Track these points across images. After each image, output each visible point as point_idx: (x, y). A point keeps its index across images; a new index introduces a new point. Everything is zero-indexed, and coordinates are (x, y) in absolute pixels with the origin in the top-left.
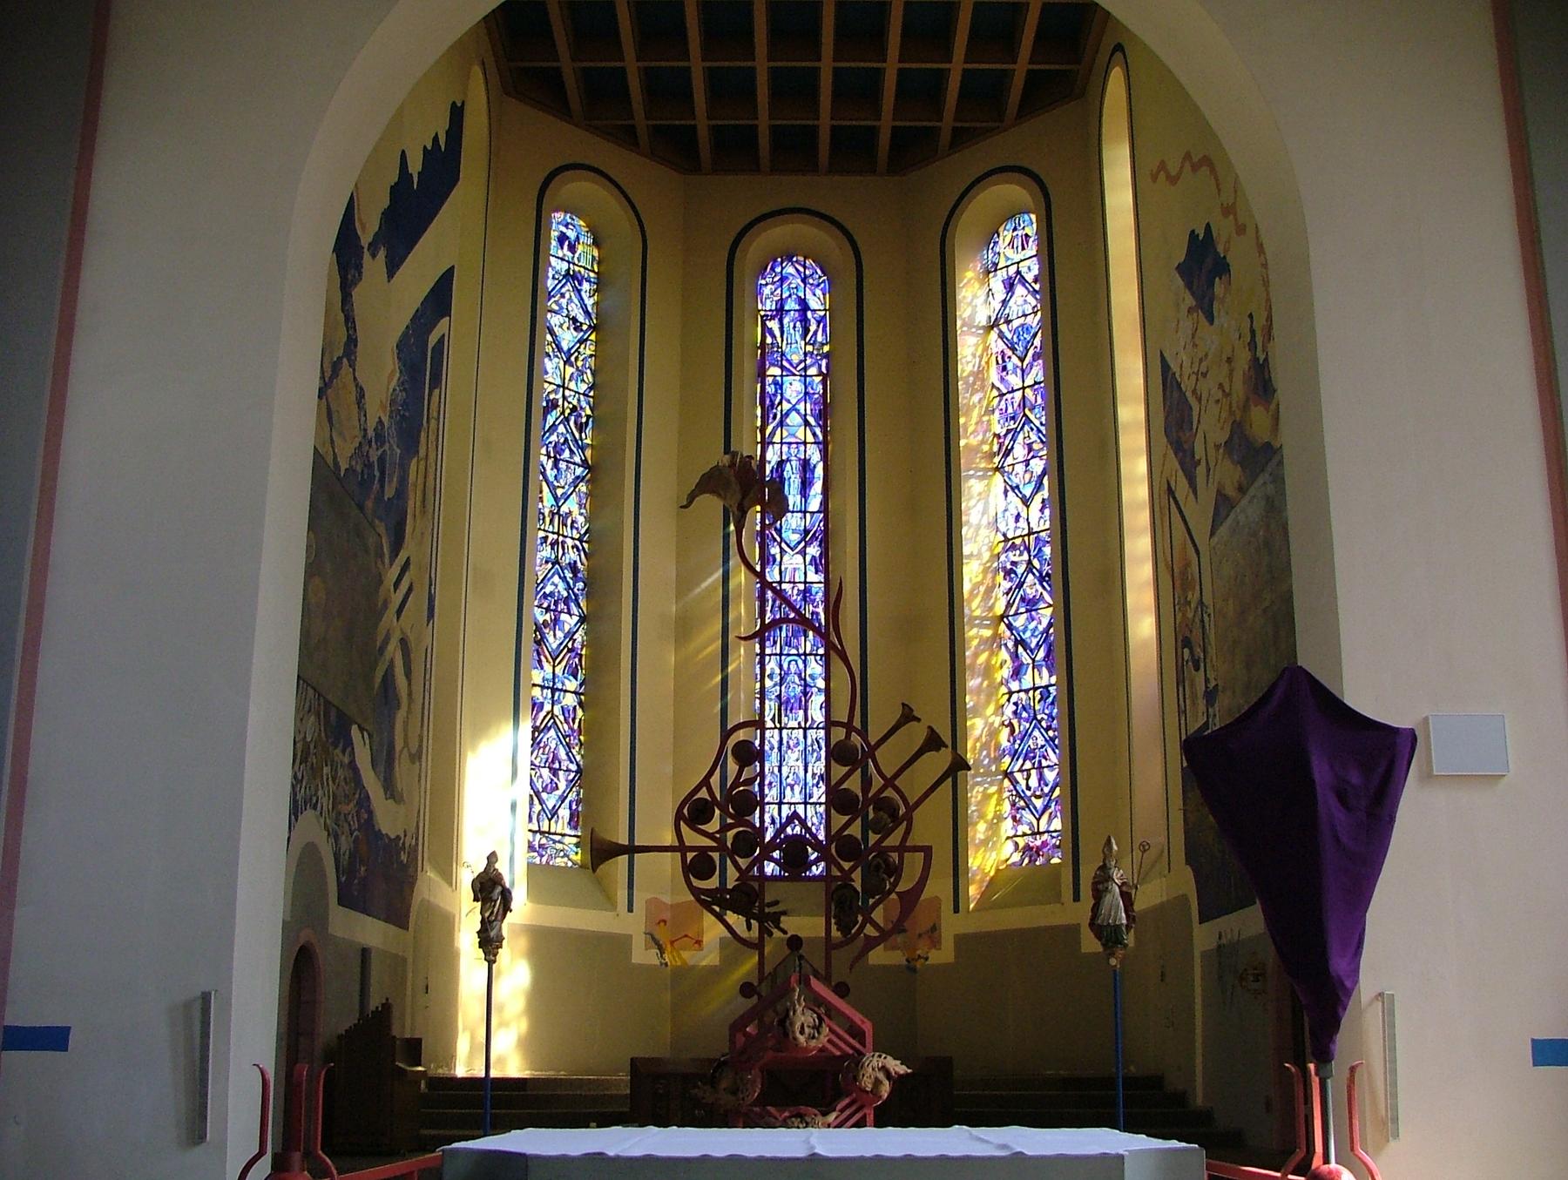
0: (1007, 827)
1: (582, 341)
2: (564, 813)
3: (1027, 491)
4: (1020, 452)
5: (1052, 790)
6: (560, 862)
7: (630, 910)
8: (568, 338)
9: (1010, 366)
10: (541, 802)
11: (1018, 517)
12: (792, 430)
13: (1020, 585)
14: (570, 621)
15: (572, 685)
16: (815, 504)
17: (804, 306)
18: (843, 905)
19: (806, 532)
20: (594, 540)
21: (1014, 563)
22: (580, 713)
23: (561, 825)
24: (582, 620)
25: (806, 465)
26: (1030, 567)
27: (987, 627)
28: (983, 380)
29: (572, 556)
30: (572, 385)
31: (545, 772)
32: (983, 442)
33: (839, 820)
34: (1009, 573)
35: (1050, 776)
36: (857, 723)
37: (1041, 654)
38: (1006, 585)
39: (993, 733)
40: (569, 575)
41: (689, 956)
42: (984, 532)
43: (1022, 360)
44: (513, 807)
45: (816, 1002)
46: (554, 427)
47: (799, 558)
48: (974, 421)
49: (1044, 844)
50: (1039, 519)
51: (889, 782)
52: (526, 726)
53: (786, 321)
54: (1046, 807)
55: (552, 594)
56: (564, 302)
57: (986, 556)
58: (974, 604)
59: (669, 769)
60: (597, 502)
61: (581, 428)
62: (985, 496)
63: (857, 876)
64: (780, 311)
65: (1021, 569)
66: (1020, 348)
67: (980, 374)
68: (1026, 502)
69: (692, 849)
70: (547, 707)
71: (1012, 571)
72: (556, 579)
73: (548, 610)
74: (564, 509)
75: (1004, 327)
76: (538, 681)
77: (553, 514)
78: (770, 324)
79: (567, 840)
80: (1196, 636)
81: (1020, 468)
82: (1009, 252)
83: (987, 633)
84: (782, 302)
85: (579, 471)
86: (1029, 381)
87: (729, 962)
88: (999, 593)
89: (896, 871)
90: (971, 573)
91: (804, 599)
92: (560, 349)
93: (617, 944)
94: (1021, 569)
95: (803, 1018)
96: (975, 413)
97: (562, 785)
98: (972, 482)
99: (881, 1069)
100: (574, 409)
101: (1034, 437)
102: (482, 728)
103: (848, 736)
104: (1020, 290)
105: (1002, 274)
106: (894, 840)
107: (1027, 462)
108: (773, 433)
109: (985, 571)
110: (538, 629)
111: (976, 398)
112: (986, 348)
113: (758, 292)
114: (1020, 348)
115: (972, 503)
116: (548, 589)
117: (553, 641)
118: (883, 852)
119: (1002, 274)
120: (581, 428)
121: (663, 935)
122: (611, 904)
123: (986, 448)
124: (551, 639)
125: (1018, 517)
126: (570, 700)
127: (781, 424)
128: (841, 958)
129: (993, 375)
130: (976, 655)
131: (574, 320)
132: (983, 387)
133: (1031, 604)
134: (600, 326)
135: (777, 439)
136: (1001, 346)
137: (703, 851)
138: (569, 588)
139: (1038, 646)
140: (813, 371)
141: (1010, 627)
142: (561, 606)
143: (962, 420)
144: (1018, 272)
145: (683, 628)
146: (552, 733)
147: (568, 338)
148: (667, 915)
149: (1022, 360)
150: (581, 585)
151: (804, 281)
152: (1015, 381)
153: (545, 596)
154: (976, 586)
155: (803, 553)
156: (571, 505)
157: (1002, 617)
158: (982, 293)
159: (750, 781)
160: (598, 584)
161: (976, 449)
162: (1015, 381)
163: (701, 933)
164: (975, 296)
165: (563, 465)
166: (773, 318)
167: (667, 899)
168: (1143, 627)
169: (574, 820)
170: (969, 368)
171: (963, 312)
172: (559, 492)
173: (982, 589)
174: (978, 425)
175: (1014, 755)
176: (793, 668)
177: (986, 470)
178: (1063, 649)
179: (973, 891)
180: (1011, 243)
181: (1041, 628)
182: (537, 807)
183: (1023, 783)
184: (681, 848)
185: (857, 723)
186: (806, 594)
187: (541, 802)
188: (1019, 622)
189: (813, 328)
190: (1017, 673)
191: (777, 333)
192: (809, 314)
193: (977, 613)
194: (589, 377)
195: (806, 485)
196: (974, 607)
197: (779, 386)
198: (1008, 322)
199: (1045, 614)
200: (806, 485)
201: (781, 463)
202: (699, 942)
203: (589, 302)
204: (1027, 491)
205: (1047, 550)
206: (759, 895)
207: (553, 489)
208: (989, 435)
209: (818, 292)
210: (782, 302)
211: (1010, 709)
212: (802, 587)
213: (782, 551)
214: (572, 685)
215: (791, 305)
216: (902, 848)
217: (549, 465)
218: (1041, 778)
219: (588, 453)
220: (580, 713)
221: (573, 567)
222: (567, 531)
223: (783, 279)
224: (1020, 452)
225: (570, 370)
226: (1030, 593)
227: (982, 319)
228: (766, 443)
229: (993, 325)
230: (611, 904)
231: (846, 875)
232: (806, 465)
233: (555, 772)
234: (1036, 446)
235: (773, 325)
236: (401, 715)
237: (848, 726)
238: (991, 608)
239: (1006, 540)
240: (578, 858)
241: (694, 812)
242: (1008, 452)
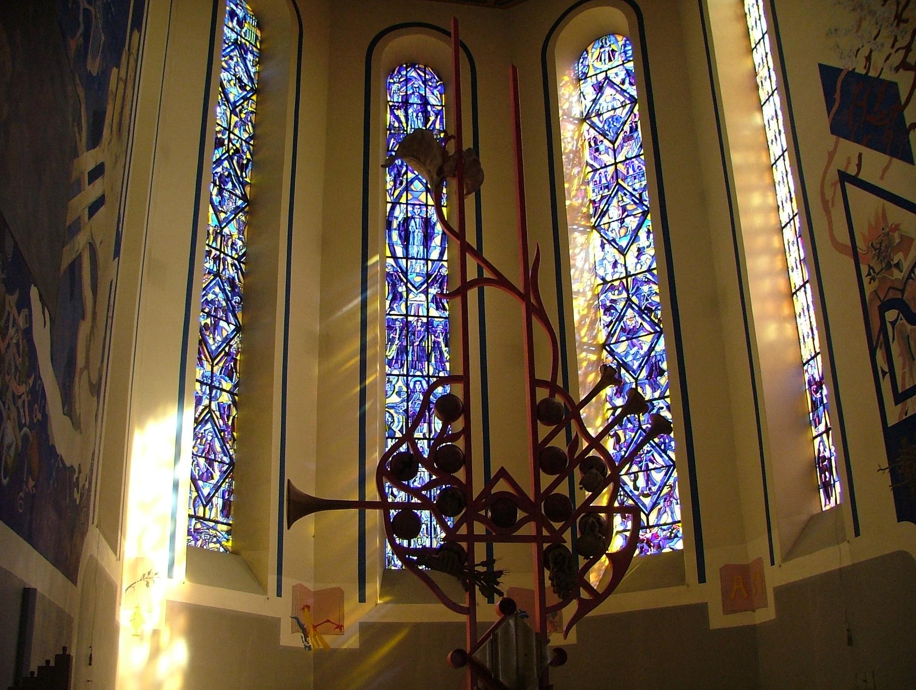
1: (245, 98)
2: (218, 501)
4: (614, 212)
5: (660, 489)
7: (279, 594)
8: (234, 93)
9: (602, 148)
10: (198, 489)
11: (615, 265)
12: (416, 194)
13: (620, 319)
14: (227, 328)
15: (227, 385)
16: (435, 255)
17: (425, 102)
19: (428, 275)
21: (613, 301)
22: (234, 412)
23: (215, 513)
24: (238, 329)
25: (427, 222)
26: (629, 303)
27: (593, 352)
28: (580, 158)
29: (231, 272)
30: (236, 131)
31: (202, 461)
32: (582, 205)
33: (547, 480)
34: (607, 310)
36: (560, 383)
37: (644, 374)
38: (608, 319)
40: (228, 288)
42: (586, 275)
43: (613, 143)
44: (176, 486)
46: (219, 162)
47: (422, 297)
48: (575, 187)
49: (656, 536)
51: (596, 443)
52: (190, 412)
53: (410, 111)
54: (655, 505)
55: (212, 302)
56: (232, 63)
57: (589, 295)
58: (583, 332)
59: (313, 467)
61: (243, 168)
62: (586, 246)
63: (567, 535)
64: (405, 104)
65: (620, 306)
66: (611, 135)
67: (577, 153)
68: (623, 251)
69: (395, 505)
70: (206, 402)
71: (611, 307)
72: (217, 290)
73: (209, 315)
74: (226, 231)
75: (595, 120)
76: (198, 377)
77: (216, 234)
78: (398, 112)
79: (220, 527)
81: (615, 225)
82: (598, 64)
83: (593, 357)
84: (406, 97)
85: (240, 202)
86: (620, 158)
88: (600, 326)
89: (607, 532)
90: (579, 307)
91: (427, 330)
92: (228, 100)
93: (266, 627)
94: (620, 306)
96: (576, 182)
97: (217, 475)
98: (576, 234)
100: (237, 151)
101: (627, 200)
102: (151, 407)
103: (552, 395)
104: (608, 91)
105: (591, 81)
106: (603, 501)
107: (622, 221)
108: (400, 196)
109: (589, 307)
110: (201, 331)
111: (575, 171)
112: (581, 135)
113: (388, 88)
114: (611, 135)
115: (577, 251)
116: (210, 297)
119: (591, 81)
120: (243, 168)
121: (307, 620)
122: (261, 587)
123: (585, 210)
124: (211, 341)
125: (615, 265)
126: (225, 398)
127: (407, 189)
129: (587, 156)
130: (586, 375)
131: (240, 80)
132: (580, 164)
134: (259, 89)
135: (403, 200)
136: (593, 133)
137: (407, 508)
138: (227, 299)
139: (640, 367)
141: (612, 353)
142: (221, 314)
143: (566, 185)
144: (607, 78)
145: (326, 345)
146: (209, 426)
147: (234, 93)
148: (310, 602)
149: (613, 143)
150: (237, 299)
151: (425, 82)
152: (608, 159)
153: (207, 302)
154: (583, 317)
155: (426, 292)
156: (231, 229)
157: (604, 346)
158: (576, 94)
159: (455, 437)
160: (251, 299)
161: (577, 210)
162: (608, 159)
163: (342, 617)
164: (570, 95)
165: (226, 194)
166: (399, 108)
167: (311, 586)
169: (226, 509)
170: (569, 147)
171: (564, 105)
172: (222, 216)
173: (588, 321)
174: (578, 193)
176: (418, 387)
177: (585, 227)
180: (599, 58)
181: (642, 352)
182: (195, 494)
183: (631, 484)
185: (560, 383)
186: (429, 326)
187: (198, 489)
188: (621, 349)
189: (432, 118)
191: (403, 119)
192: (429, 108)
193: (585, 340)
194: (250, 128)
195: (427, 239)
196: (583, 335)
198: (599, 115)
200: (427, 239)
201: (407, 220)
202: (340, 627)
203: (252, 70)
204: (623, 243)
207: (216, 212)
208: (586, 201)
209: (436, 92)
210: (406, 97)
212: (425, 320)
213: (408, 291)
214: (227, 385)
215: (414, 99)
217: (215, 191)
218: (648, 479)
219: (248, 189)
220: (234, 412)
221: (231, 281)
222: (228, 251)
223: (408, 80)
224: (614, 212)
225: (235, 119)
226: (630, 324)
227: (577, 111)
228: (394, 204)
229: (586, 118)
231: (556, 537)
232: (427, 222)
233: (210, 462)
234: (629, 207)
235: (400, 113)
236: (84, 328)
237: (551, 385)
238: (595, 337)
239: (605, 282)
240: (230, 544)
242: (604, 214)
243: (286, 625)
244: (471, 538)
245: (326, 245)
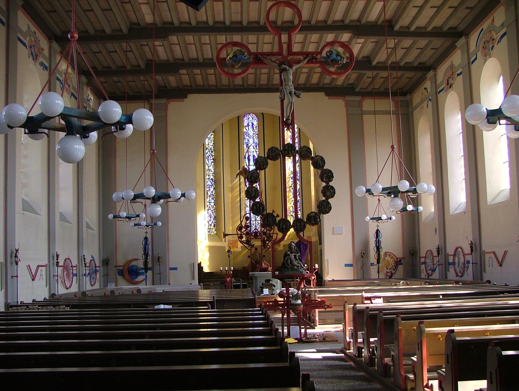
2: (213, 225)
6: (212, 234)
14: (212, 189)
15: (213, 201)
17: (252, 123)
18: (264, 242)
20: (215, 174)
33: (263, 229)
45: (264, 263)
60: (216, 166)
61: (212, 152)
64: (248, 125)
85: (212, 161)
87: (243, 250)
89: (272, 237)
95: (263, 264)
97: (212, 220)
106: (272, 232)
113: (243, 122)
117: (209, 193)
118: (270, 234)
120: (212, 152)
126: (213, 204)
128: (264, 251)
140: (255, 137)
145: (232, 189)
160: (217, 182)
167: (231, 239)
169: (214, 227)
184: (238, 234)
194: (213, 142)
197: (248, 140)
215: (250, 124)
216: (273, 233)
221: (212, 179)
230: (222, 241)
241: (240, 228)
244: (251, 239)
245: (231, 166)
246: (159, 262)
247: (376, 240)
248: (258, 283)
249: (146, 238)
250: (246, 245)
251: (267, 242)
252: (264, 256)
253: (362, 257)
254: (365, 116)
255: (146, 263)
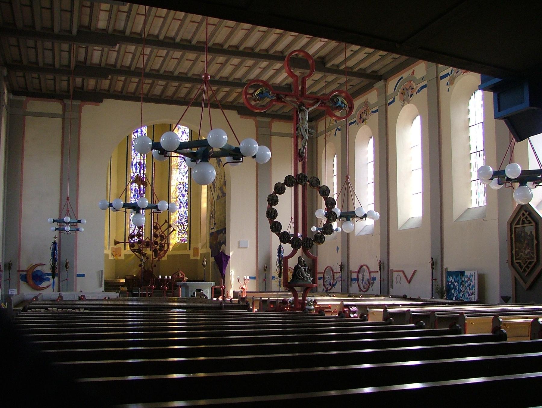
0: (177, 235)
3: (184, 174)
4: (183, 166)
18: (155, 251)
26: (183, 188)
34: (179, 189)
35: (186, 227)
37: (185, 205)
39: (175, 218)
41: (119, 258)
50: (187, 180)
51: (163, 233)
65: (182, 188)
80: (213, 214)
89: (164, 247)
90: (173, 189)
94: (182, 188)
99: (186, 278)
106: (163, 242)
133: (183, 195)
168: (204, 205)
175: (179, 223)
178: (189, 204)
179: (171, 247)
188: (181, 198)
190: (180, 208)
196: (173, 195)
199: (186, 198)
204: (184, 174)
205: (187, 186)
206: (142, 251)
211: (178, 214)
216: (165, 243)
218: (184, 227)
224: (183, 166)
235: (136, 134)
243: (110, 255)
244: (142, 248)
245: (118, 172)
246: (67, 268)
247: (279, 255)
248: (190, 292)
249: (55, 243)
250: (137, 254)
251: (159, 252)
252: (155, 266)
253: (265, 270)
254: (273, 137)
255: (53, 268)
